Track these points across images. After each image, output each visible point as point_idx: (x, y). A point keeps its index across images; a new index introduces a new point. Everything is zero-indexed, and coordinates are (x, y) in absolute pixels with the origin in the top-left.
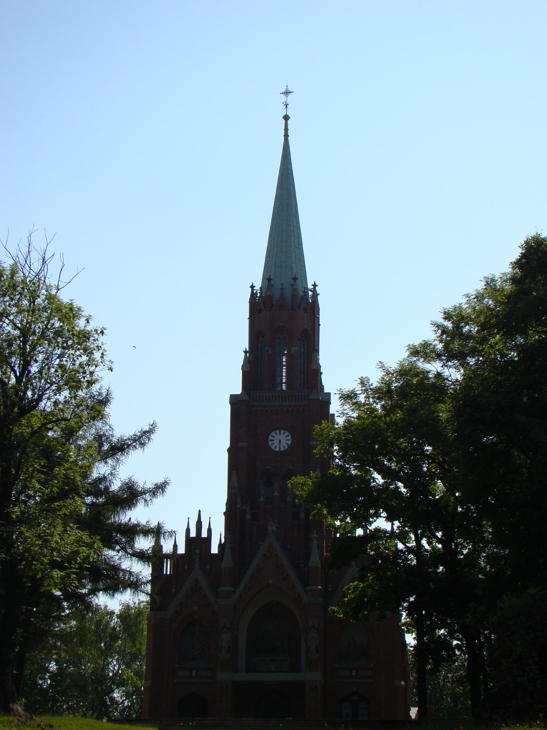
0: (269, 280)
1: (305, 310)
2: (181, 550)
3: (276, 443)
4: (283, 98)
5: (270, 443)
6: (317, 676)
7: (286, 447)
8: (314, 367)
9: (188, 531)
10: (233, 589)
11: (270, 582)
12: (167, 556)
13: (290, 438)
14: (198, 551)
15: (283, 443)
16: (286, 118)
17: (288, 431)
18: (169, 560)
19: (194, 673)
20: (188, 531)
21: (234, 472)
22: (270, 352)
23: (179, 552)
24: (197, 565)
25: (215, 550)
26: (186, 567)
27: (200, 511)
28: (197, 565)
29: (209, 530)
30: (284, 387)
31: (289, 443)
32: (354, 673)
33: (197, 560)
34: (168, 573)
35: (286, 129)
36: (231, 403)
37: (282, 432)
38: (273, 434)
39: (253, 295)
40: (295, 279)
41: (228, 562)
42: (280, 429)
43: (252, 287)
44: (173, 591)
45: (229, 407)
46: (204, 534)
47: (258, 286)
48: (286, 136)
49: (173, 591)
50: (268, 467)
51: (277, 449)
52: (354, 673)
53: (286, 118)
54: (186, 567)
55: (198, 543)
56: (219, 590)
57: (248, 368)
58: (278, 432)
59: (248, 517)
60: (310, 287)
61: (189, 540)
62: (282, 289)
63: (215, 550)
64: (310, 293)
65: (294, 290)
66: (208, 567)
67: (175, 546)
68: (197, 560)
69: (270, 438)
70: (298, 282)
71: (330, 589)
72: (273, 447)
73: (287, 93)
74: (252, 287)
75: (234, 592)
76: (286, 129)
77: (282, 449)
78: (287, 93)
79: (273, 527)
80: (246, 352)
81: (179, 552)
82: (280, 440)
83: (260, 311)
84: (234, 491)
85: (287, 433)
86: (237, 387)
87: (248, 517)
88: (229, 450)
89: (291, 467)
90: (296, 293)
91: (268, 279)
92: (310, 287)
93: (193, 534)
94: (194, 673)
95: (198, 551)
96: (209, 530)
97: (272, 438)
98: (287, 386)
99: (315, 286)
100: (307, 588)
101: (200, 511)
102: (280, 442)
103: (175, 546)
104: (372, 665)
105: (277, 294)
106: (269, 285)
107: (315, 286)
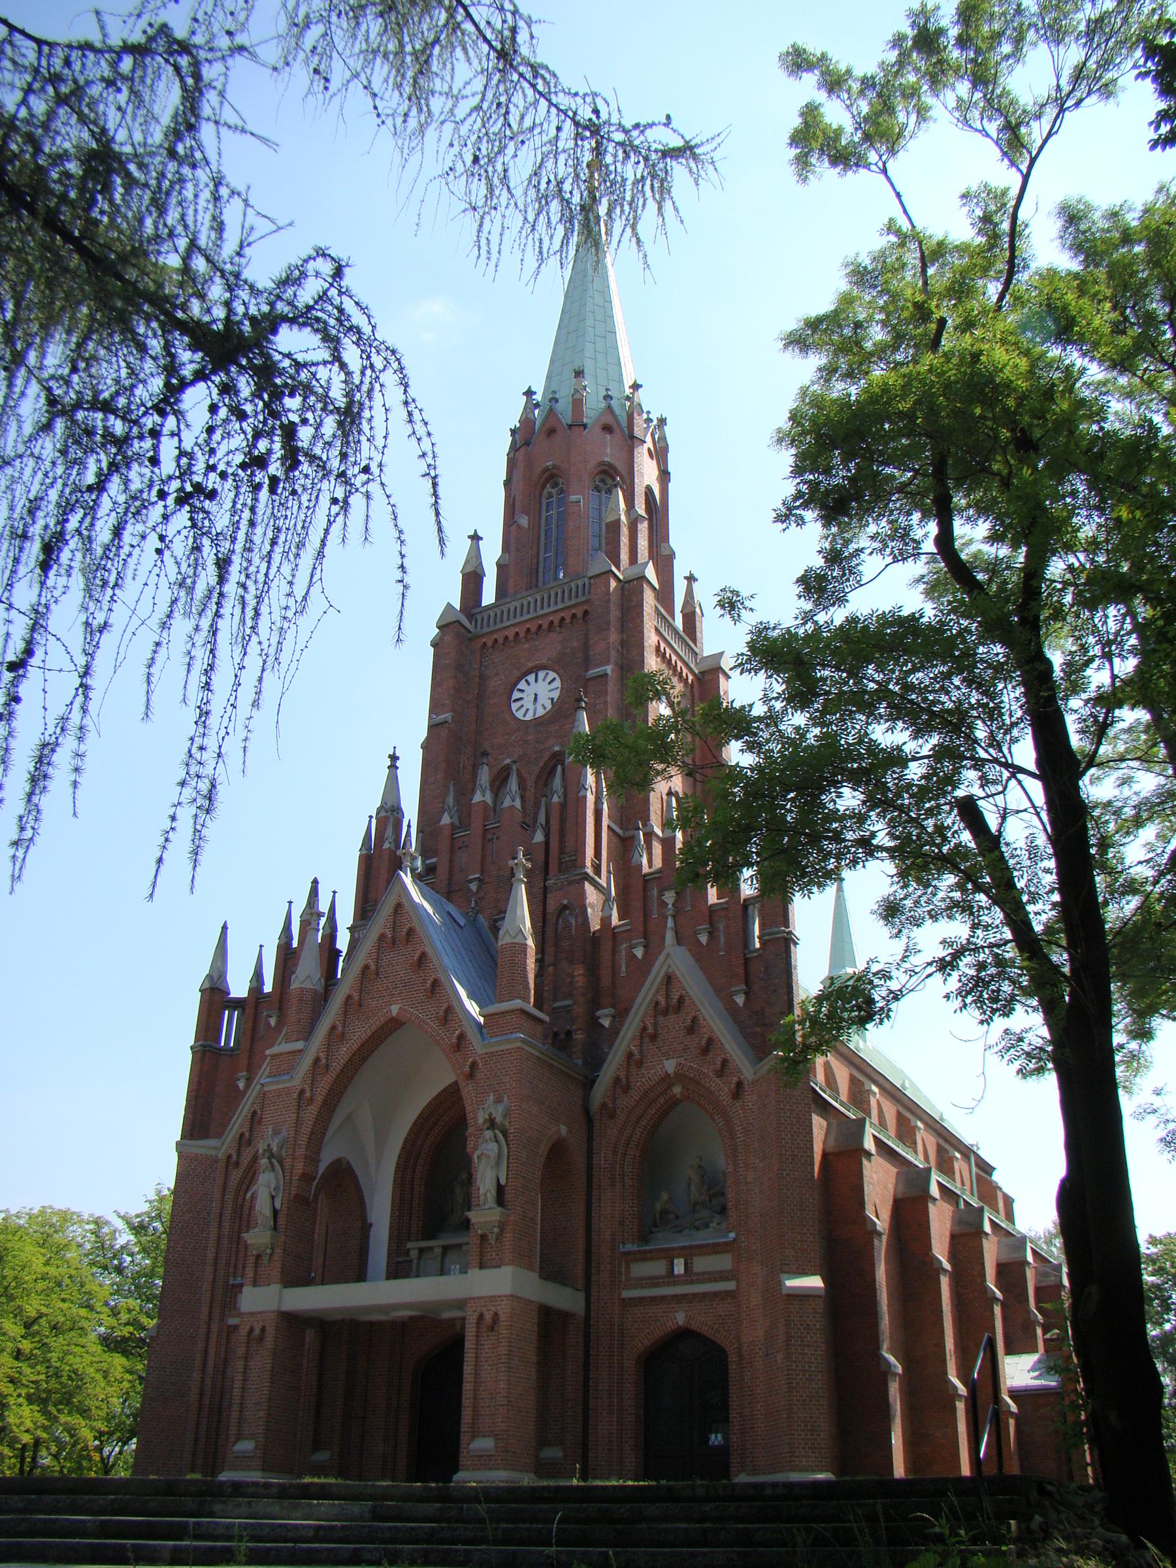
3: (528, 702)
5: (514, 706)
7: (549, 706)
11: (395, 1010)
12: (238, 1004)
13: (558, 683)
15: (540, 701)
31: (556, 695)
32: (679, 1267)
37: (541, 674)
38: (522, 685)
42: (535, 670)
49: (241, 1085)
51: (529, 717)
52: (679, 1267)
58: (531, 678)
65: (593, 405)
67: (258, 975)
71: (606, 1023)
77: (540, 712)
82: (537, 695)
85: (552, 675)
99: (636, 387)
103: (258, 975)
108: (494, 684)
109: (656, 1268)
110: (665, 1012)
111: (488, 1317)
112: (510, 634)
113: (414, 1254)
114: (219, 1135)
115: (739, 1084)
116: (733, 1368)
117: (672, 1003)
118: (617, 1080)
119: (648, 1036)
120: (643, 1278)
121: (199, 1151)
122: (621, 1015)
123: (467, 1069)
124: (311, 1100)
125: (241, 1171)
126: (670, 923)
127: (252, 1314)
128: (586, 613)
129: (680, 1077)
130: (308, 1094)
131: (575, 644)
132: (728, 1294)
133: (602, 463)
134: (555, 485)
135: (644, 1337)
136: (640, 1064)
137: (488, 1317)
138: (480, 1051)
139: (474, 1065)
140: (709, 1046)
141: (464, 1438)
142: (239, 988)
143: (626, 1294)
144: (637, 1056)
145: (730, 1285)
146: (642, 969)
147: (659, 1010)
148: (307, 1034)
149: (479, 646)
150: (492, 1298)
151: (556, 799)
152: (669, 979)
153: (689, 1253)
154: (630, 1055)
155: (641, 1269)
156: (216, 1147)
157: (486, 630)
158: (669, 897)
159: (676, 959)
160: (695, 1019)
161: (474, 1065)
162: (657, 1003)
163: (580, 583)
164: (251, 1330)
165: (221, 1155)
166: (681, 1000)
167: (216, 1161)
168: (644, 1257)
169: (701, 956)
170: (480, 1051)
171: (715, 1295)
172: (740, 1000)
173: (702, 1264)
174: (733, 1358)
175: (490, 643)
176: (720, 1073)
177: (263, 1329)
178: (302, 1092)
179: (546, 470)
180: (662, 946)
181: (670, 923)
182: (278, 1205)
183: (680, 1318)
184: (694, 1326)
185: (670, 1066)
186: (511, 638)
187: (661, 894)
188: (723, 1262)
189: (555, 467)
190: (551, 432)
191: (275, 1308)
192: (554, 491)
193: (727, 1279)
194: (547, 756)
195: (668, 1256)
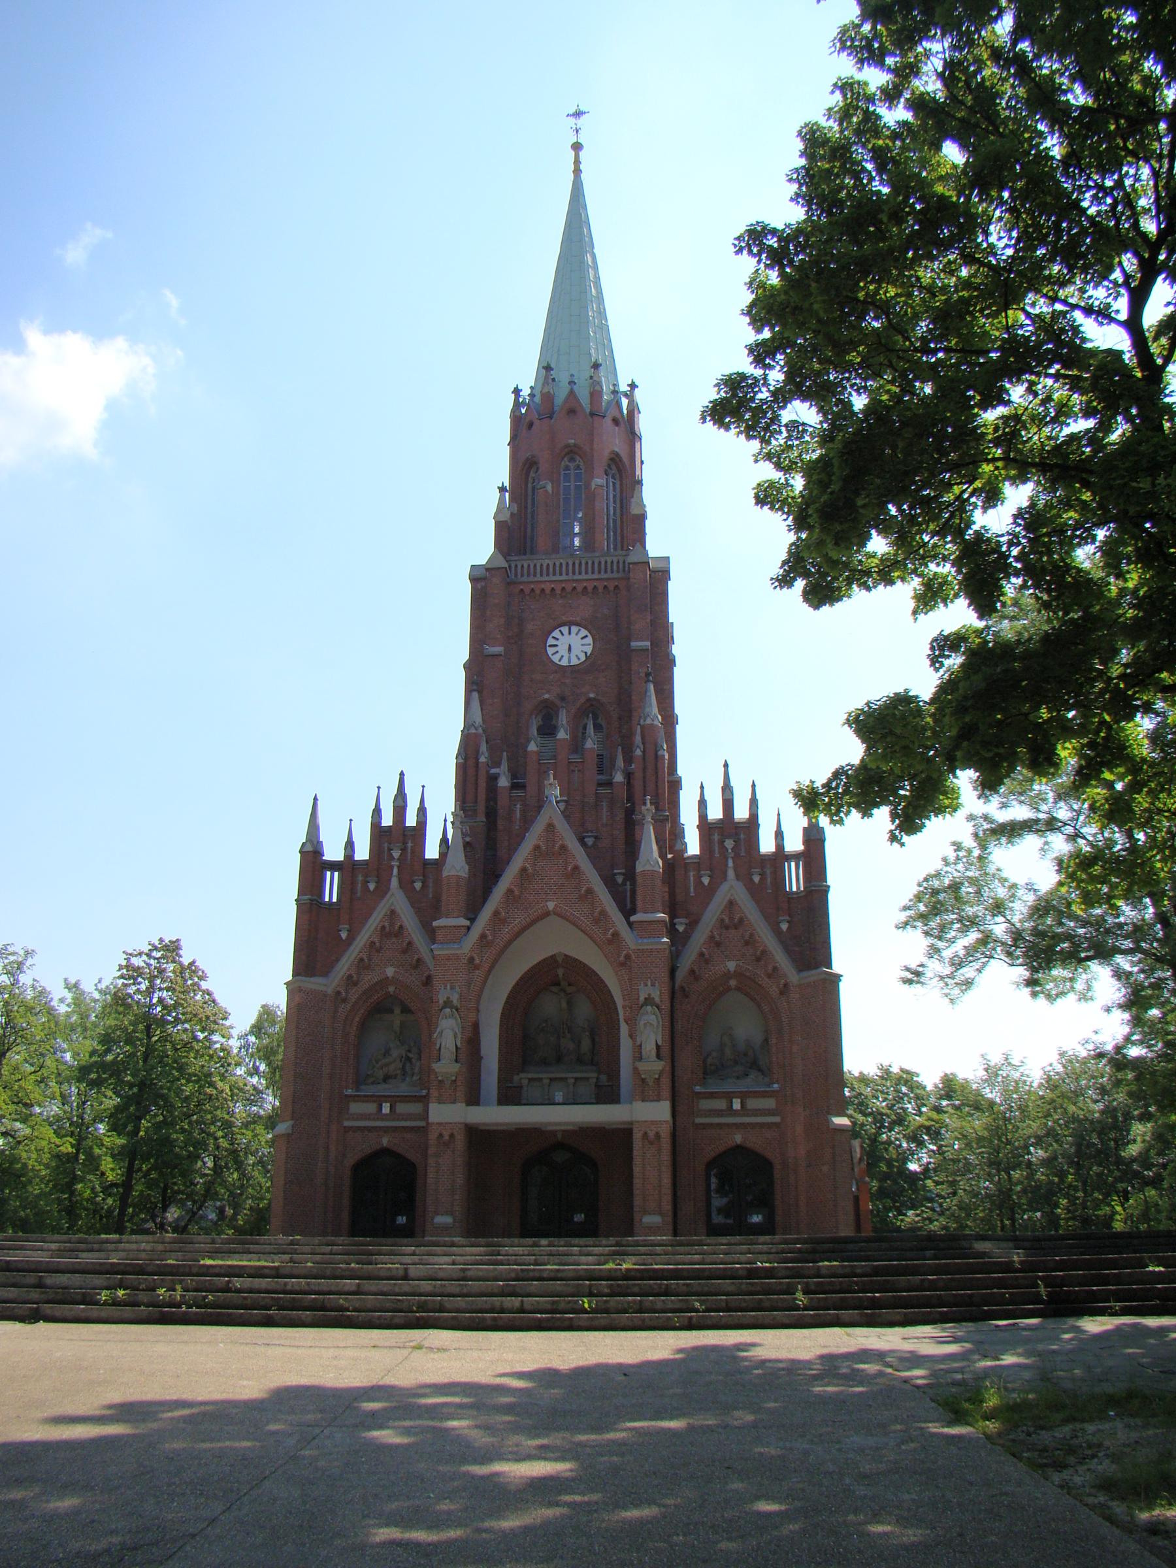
0: (548, 368)
1: (616, 422)
2: (362, 852)
4: (572, 120)
5: (550, 651)
6: (658, 1112)
7: (583, 658)
8: (635, 511)
9: (377, 812)
10: (468, 923)
11: (551, 905)
12: (333, 866)
13: (589, 640)
14: (396, 854)
15: (574, 652)
16: (577, 147)
17: (586, 628)
18: (336, 874)
19: (386, 1108)
20: (377, 812)
21: (475, 695)
22: (549, 488)
23: (357, 857)
24: (394, 882)
25: (432, 851)
26: (372, 886)
27: (402, 774)
28: (394, 882)
29: (422, 811)
30: (577, 542)
31: (589, 650)
32: (737, 1104)
33: (395, 871)
34: (335, 900)
35: (577, 162)
36: (474, 579)
37: (574, 629)
38: (556, 633)
39: (517, 404)
40: (596, 366)
41: (458, 866)
42: (570, 624)
43: (517, 391)
44: (344, 935)
45: (468, 586)
46: (411, 820)
47: (526, 392)
48: (577, 171)
49: (344, 935)
50: (547, 696)
51: (564, 663)
52: (737, 1104)
53: (577, 147)
54: (372, 886)
55: (396, 839)
56: (435, 924)
57: (506, 516)
58: (565, 629)
59: (504, 782)
60: (623, 387)
61: (379, 834)
62: (572, 383)
63: (432, 851)
64: (625, 402)
65: (595, 394)
66: (418, 885)
67: (350, 845)
68: (395, 871)
69: (551, 641)
70: (602, 372)
71: (681, 928)
72: (555, 659)
73: (578, 114)
74: (517, 391)
75: (469, 928)
76: (577, 162)
77: (574, 662)
78: (578, 114)
79: (555, 792)
80: (502, 489)
81: (357, 857)
82: (571, 646)
83: (531, 425)
84: (473, 731)
85: (584, 632)
86: (482, 548)
87: (504, 782)
88: (467, 667)
89: (592, 695)
90: (598, 388)
91: (546, 368)
92: (623, 387)
93: (387, 820)
94: (386, 1108)
95: (396, 854)
96: (422, 811)
97: (555, 642)
98: (582, 542)
99: (633, 386)
100: (632, 918)
101: (402, 774)
102: (570, 649)
103: (350, 845)
104: (776, 1086)
105: (561, 395)
106: (546, 378)
107: (633, 386)
108: (530, 627)
109: (721, 1104)
110: (727, 928)
111: (651, 1134)
112: (547, 587)
113: (525, 1082)
114: (325, 974)
115: (786, 985)
116: (777, 1175)
117: (732, 921)
118: (692, 972)
119: (714, 942)
120: (710, 1111)
121: (313, 987)
122: (693, 924)
123: (622, 958)
124: (477, 967)
125: (349, 1006)
126: (730, 863)
127: (440, 1124)
128: (616, 587)
129: (738, 974)
130: (477, 961)
131: (606, 612)
132: (777, 1125)
133: (613, 452)
134: (572, 460)
135: (711, 1152)
136: (707, 962)
137: (651, 1134)
138: (632, 946)
139: (628, 957)
140: (762, 957)
141: (637, 1217)
142: (333, 852)
143: (698, 1120)
144: (707, 956)
145: (777, 1119)
146: (711, 891)
147: (723, 925)
148: (472, 914)
149: (517, 591)
150: (653, 1123)
151: (638, 752)
152: (731, 903)
153: (744, 1096)
154: (701, 954)
155: (705, 1104)
156: (315, 983)
157: (525, 579)
158: (729, 844)
159: (732, 889)
160: (752, 935)
161: (628, 957)
162: (722, 920)
163: (609, 560)
164: (441, 1135)
165: (330, 991)
166: (741, 920)
167: (325, 995)
168: (712, 1096)
169: (755, 891)
170: (632, 946)
171: (762, 1125)
172: (784, 926)
173: (752, 1104)
174: (777, 1167)
175: (527, 591)
176: (769, 976)
177: (452, 1136)
178: (471, 960)
179: (567, 446)
180: (725, 878)
181: (730, 863)
182: (459, 1045)
183: (738, 1139)
184: (749, 1145)
185: (731, 966)
186: (548, 592)
187: (722, 842)
188: (770, 1103)
189: (575, 445)
190: (572, 412)
191: (462, 1120)
192: (572, 465)
193: (773, 1115)
194: (582, 700)
195: (729, 1097)
